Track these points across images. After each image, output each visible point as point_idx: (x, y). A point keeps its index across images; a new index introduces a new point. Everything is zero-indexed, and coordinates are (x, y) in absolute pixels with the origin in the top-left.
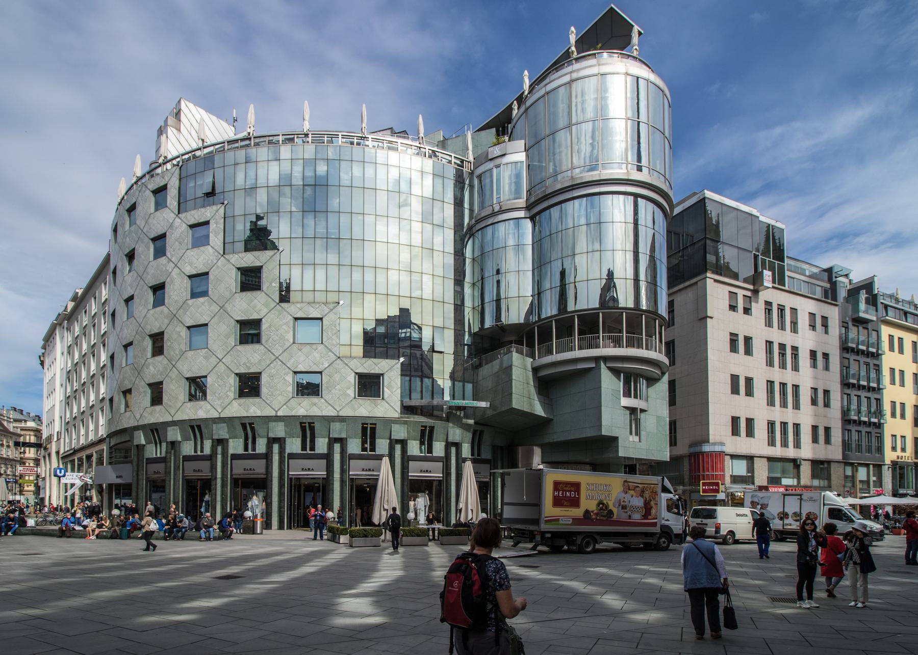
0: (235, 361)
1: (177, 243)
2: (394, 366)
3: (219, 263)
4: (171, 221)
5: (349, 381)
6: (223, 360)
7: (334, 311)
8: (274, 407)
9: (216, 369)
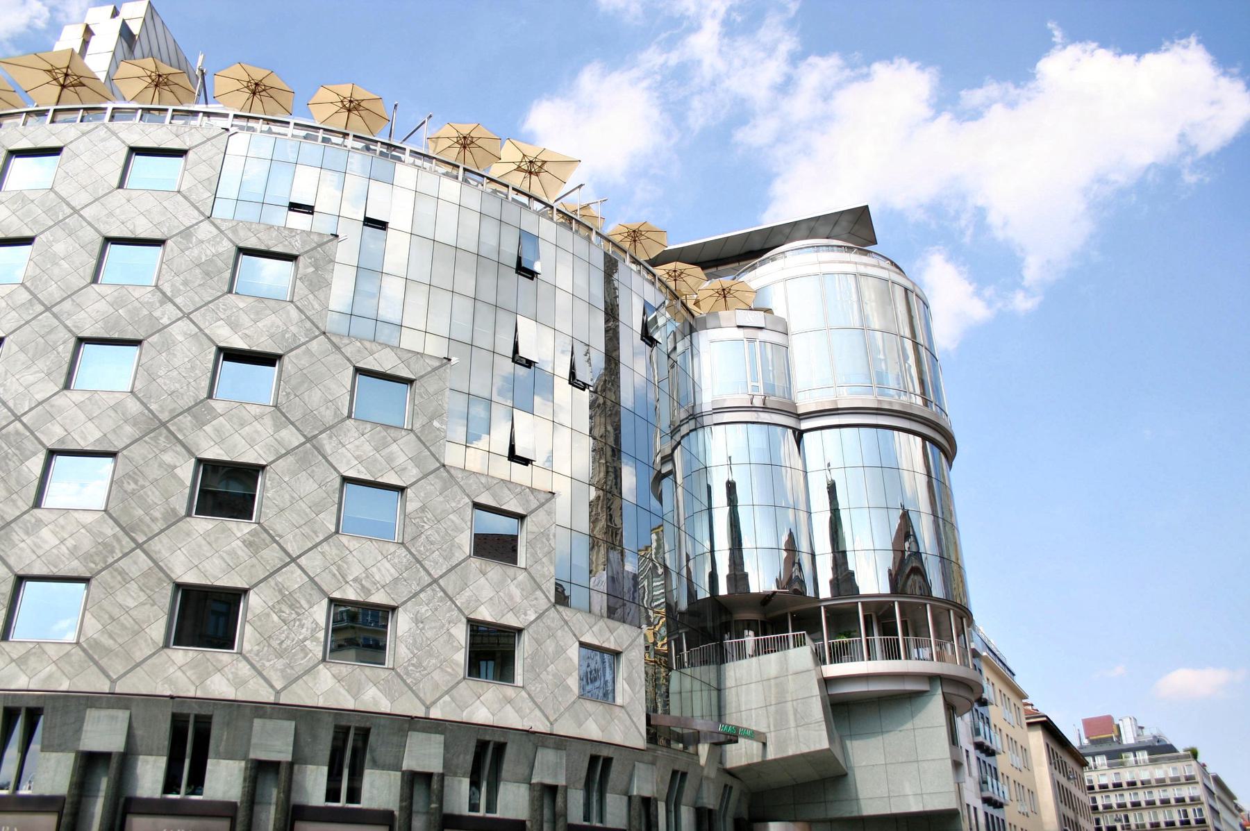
0: (334, 569)
1: (198, 271)
2: (635, 640)
3: (314, 346)
4: (188, 224)
5: (571, 659)
6: (302, 561)
7: (545, 507)
8: (421, 695)
9: (279, 578)
